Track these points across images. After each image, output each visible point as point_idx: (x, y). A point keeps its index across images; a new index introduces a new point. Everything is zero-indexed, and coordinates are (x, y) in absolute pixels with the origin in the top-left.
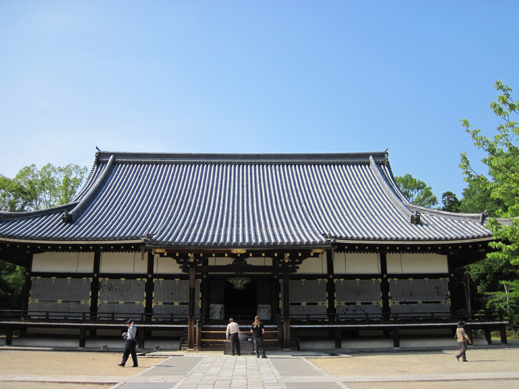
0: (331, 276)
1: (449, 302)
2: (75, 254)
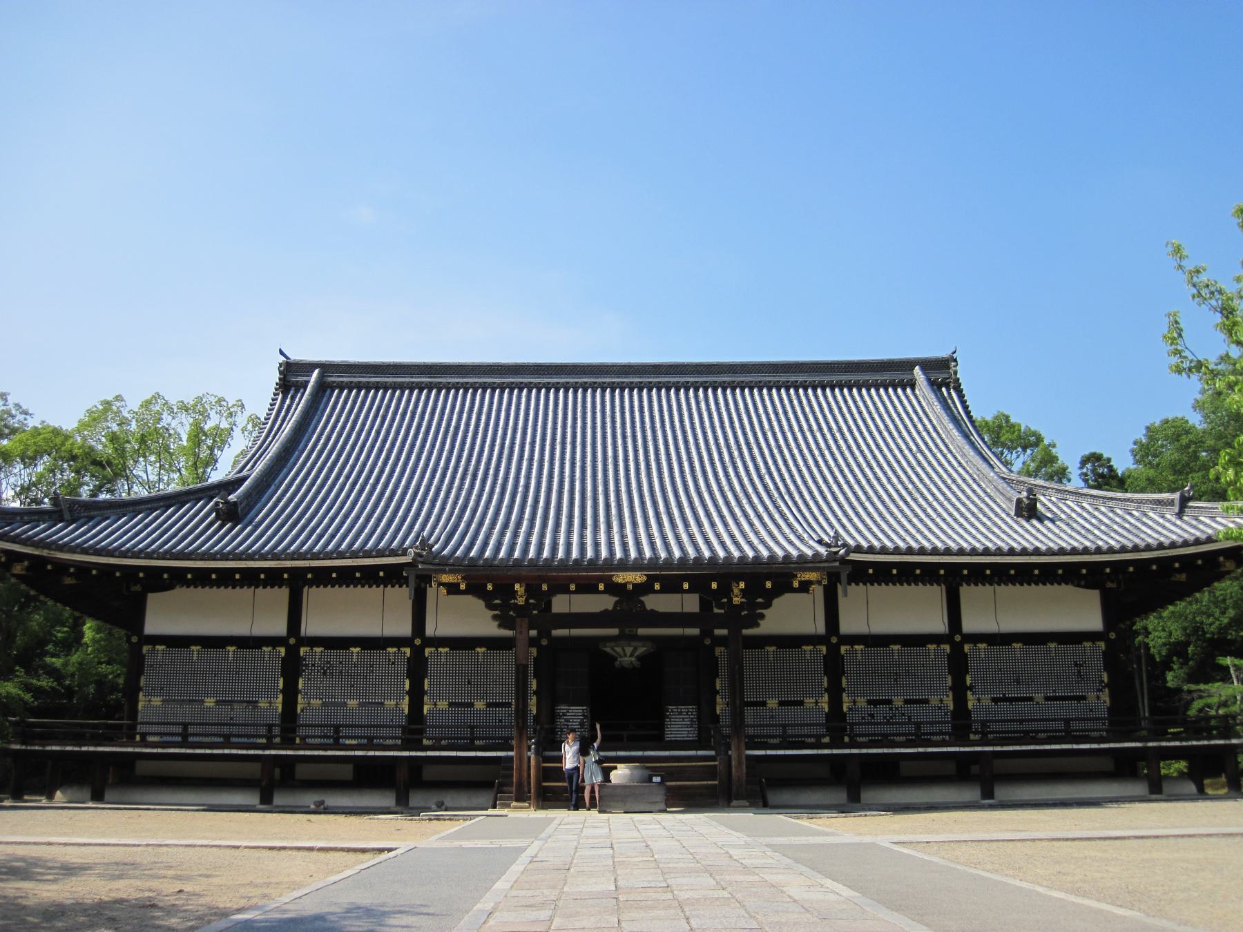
0: (834, 640)
1: (1105, 696)
2: (246, 593)
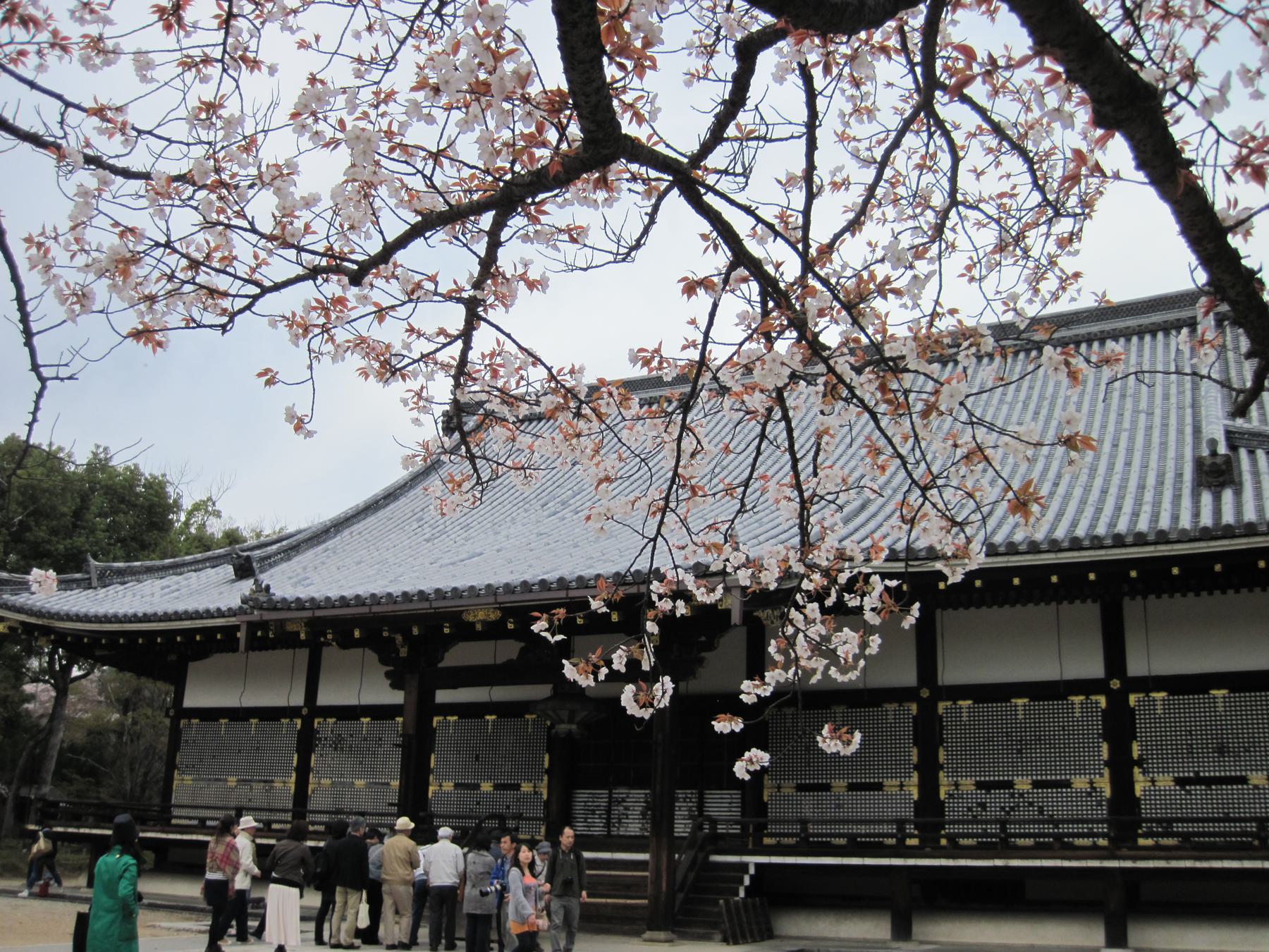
0: (1115, 684)
